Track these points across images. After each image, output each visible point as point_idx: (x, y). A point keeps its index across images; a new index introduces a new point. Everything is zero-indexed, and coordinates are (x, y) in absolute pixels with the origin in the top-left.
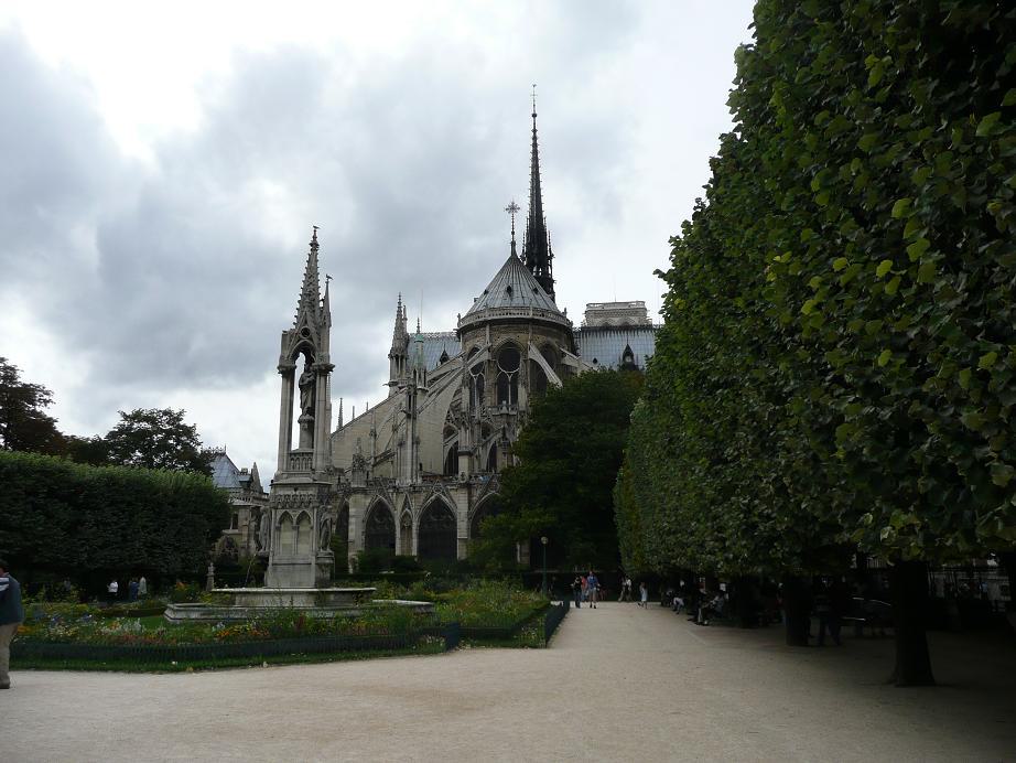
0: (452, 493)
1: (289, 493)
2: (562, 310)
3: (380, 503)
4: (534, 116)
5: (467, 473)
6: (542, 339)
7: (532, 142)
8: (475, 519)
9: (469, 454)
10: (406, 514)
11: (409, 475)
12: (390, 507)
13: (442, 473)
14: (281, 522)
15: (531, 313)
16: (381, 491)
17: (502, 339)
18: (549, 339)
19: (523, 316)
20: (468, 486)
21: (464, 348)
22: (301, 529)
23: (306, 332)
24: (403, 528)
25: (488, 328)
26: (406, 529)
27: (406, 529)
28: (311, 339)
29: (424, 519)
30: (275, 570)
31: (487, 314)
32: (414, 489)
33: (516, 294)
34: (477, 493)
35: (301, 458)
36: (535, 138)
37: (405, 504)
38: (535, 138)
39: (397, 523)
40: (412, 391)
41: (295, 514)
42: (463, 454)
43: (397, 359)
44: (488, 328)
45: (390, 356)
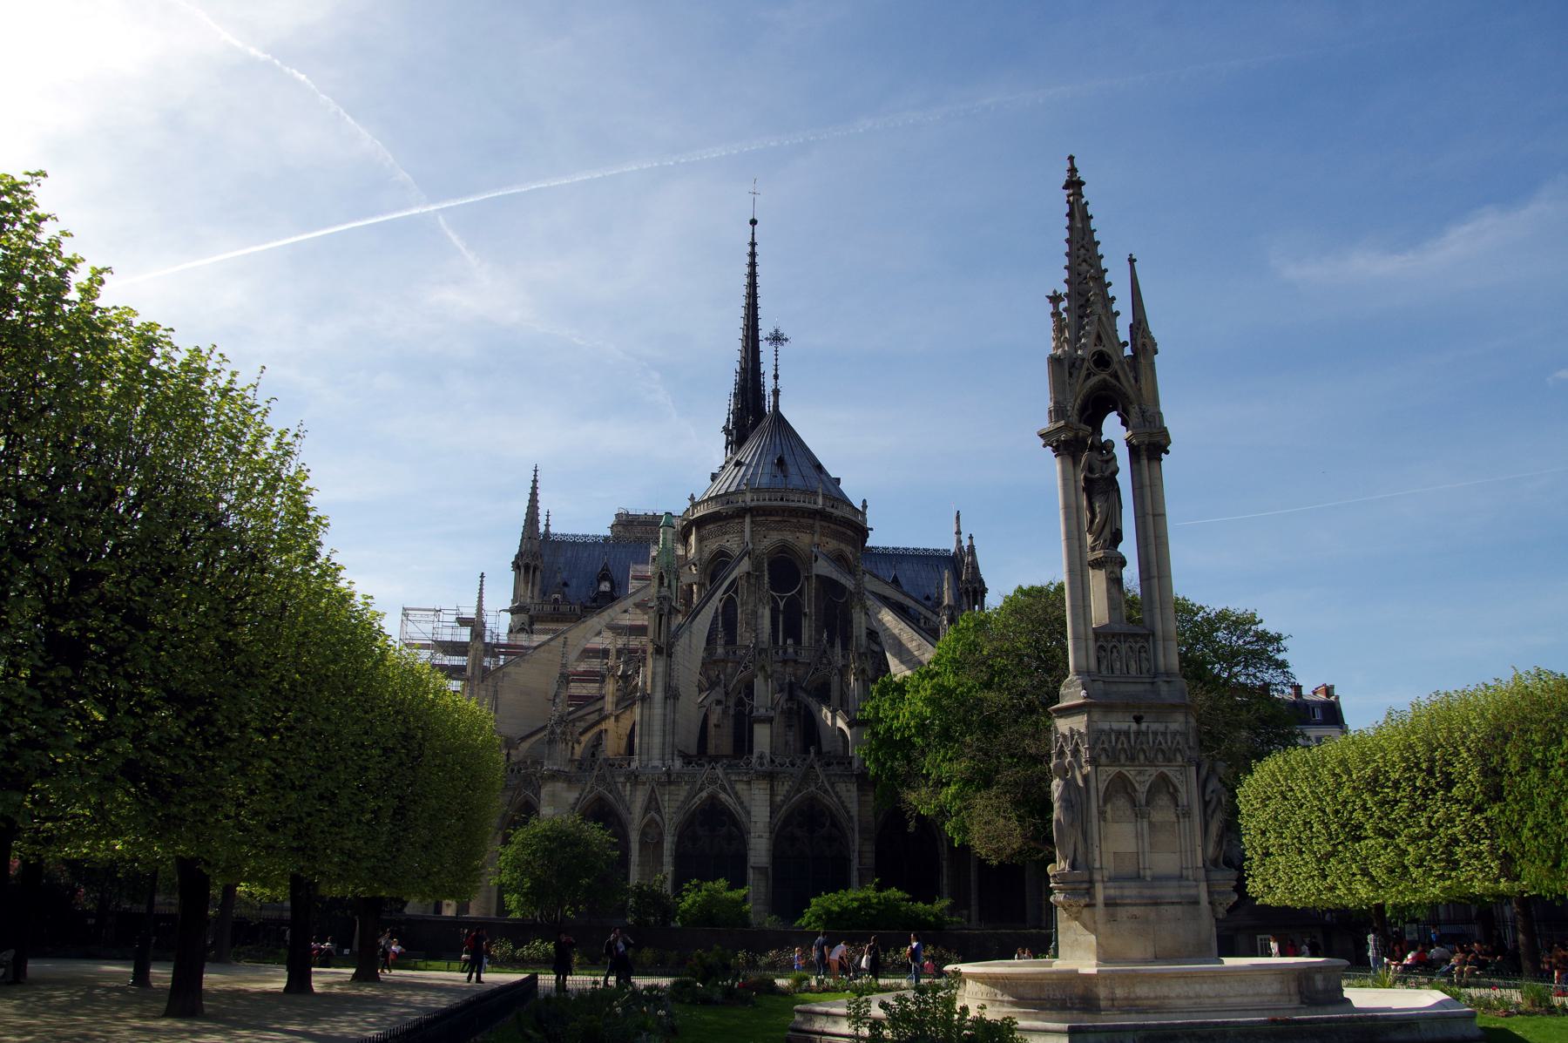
0: (739, 787)
1: (1124, 726)
2: (859, 506)
3: (600, 799)
4: (753, 222)
5: (767, 752)
6: (833, 545)
7: (748, 260)
8: (781, 837)
9: (770, 720)
10: (653, 820)
11: (656, 752)
12: (621, 809)
13: (693, 750)
14: (1107, 798)
15: (820, 501)
16: (601, 779)
17: (771, 540)
18: (843, 546)
19: (806, 505)
20: (771, 777)
21: (700, 550)
22: (1157, 816)
23: (1102, 360)
24: (643, 844)
25: (748, 520)
26: (651, 844)
27: (651, 844)
28: (1116, 377)
29: (686, 833)
30: (1112, 919)
31: (748, 497)
32: (670, 779)
33: (792, 469)
34: (783, 789)
35: (1124, 647)
36: (753, 255)
37: (650, 802)
38: (753, 255)
39: (634, 838)
40: (666, 610)
41: (1140, 779)
42: (761, 720)
43: (527, 571)
44: (748, 520)
45: (516, 566)
